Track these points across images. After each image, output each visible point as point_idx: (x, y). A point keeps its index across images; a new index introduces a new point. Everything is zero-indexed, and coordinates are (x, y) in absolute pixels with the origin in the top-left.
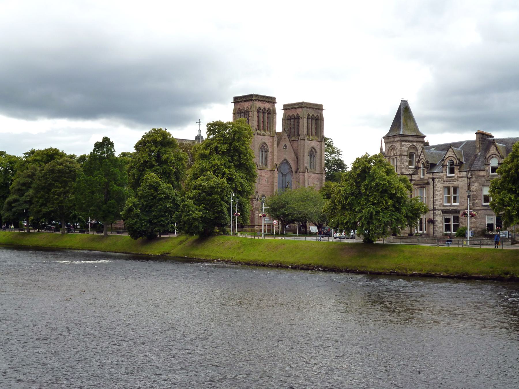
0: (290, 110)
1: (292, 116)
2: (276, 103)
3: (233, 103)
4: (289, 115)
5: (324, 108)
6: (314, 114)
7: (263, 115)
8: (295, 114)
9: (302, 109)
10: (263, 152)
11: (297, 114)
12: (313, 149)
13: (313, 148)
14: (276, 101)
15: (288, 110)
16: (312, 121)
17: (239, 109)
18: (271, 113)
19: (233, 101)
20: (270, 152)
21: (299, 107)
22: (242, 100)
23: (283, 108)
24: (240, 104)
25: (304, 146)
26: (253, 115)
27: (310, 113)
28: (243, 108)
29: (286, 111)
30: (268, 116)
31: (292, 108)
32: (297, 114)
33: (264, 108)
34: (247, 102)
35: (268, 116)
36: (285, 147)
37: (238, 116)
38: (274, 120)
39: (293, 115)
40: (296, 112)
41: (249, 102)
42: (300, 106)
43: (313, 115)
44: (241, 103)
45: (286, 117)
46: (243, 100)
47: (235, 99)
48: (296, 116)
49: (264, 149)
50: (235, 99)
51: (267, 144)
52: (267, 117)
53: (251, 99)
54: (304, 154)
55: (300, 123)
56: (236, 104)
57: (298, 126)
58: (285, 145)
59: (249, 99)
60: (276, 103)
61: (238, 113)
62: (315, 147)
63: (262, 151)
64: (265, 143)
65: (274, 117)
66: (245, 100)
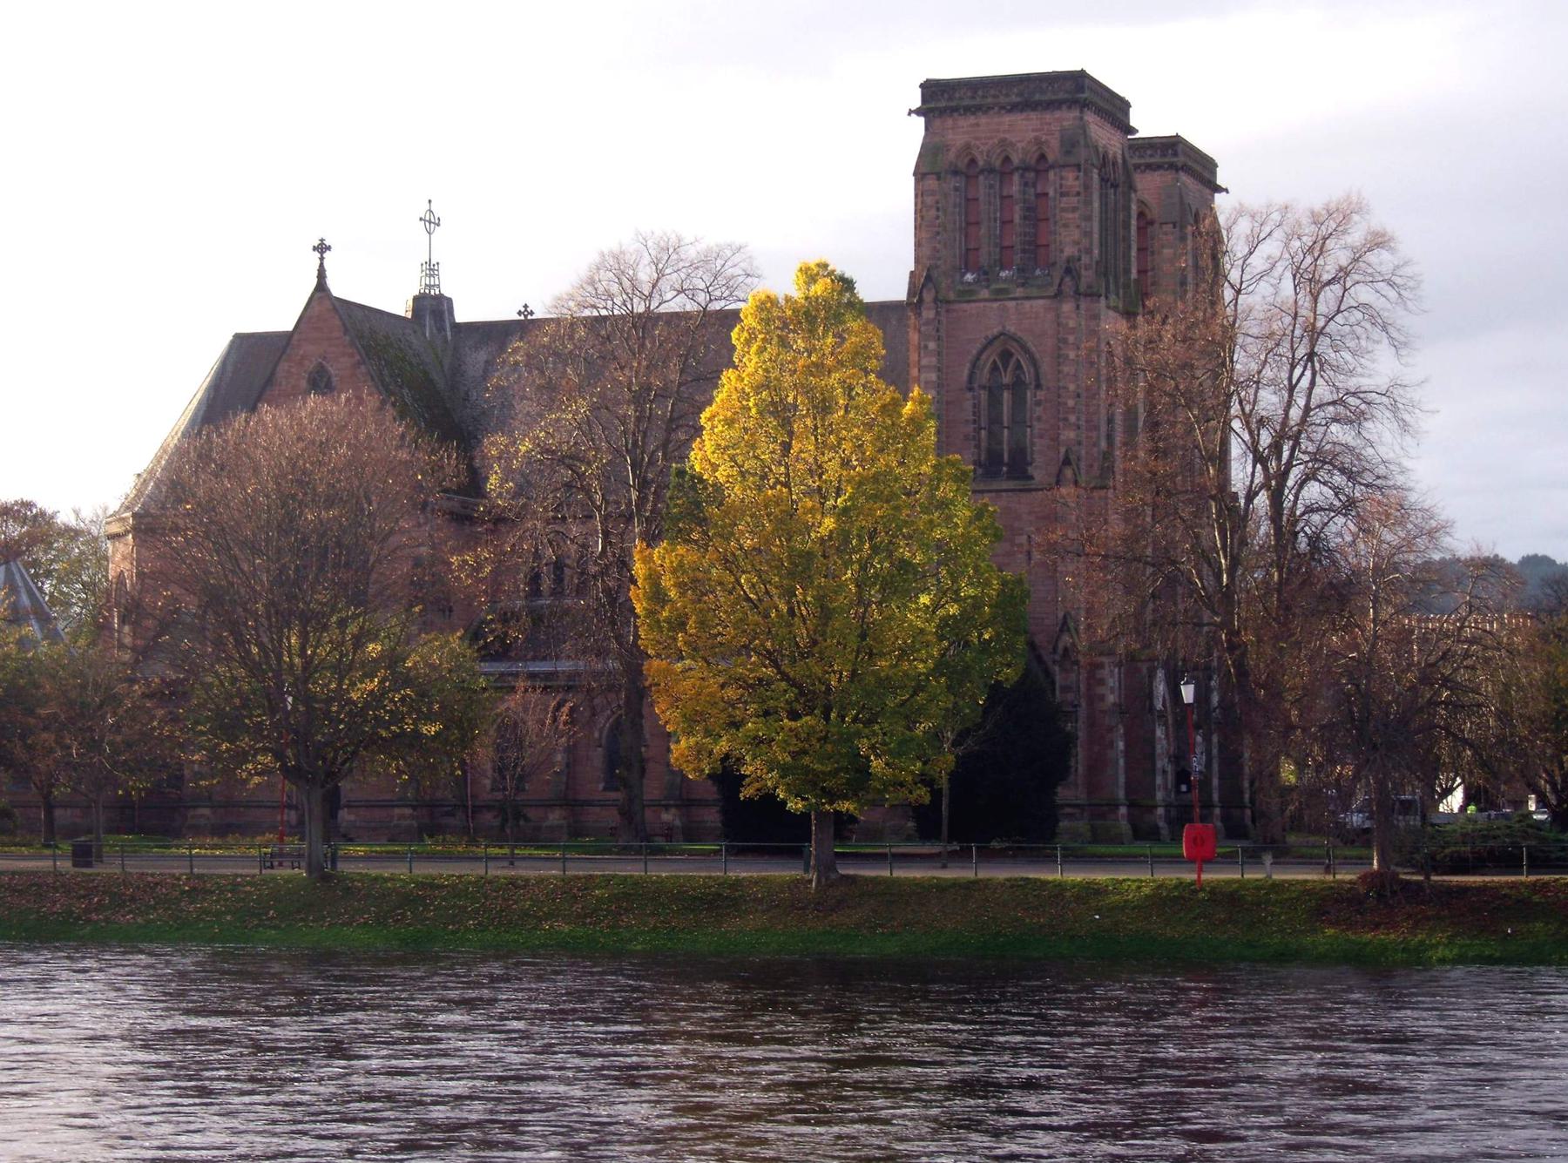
3: (918, 112)
9: (1169, 176)
17: (968, 147)
19: (917, 103)
22: (990, 100)
24: (972, 120)
26: (1087, 187)
28: (1003, 141)
34: (1033, 115)
37: (956, 189)
41: (1048, 116)
42: (1157, 159)
46: (1002, 100)
47: (932, 89)
50: (932, 89)
53: (1061, 96)
56: (937, 123)
59: (1049, 96)
61: (956, 173)
66: (1015, 99)
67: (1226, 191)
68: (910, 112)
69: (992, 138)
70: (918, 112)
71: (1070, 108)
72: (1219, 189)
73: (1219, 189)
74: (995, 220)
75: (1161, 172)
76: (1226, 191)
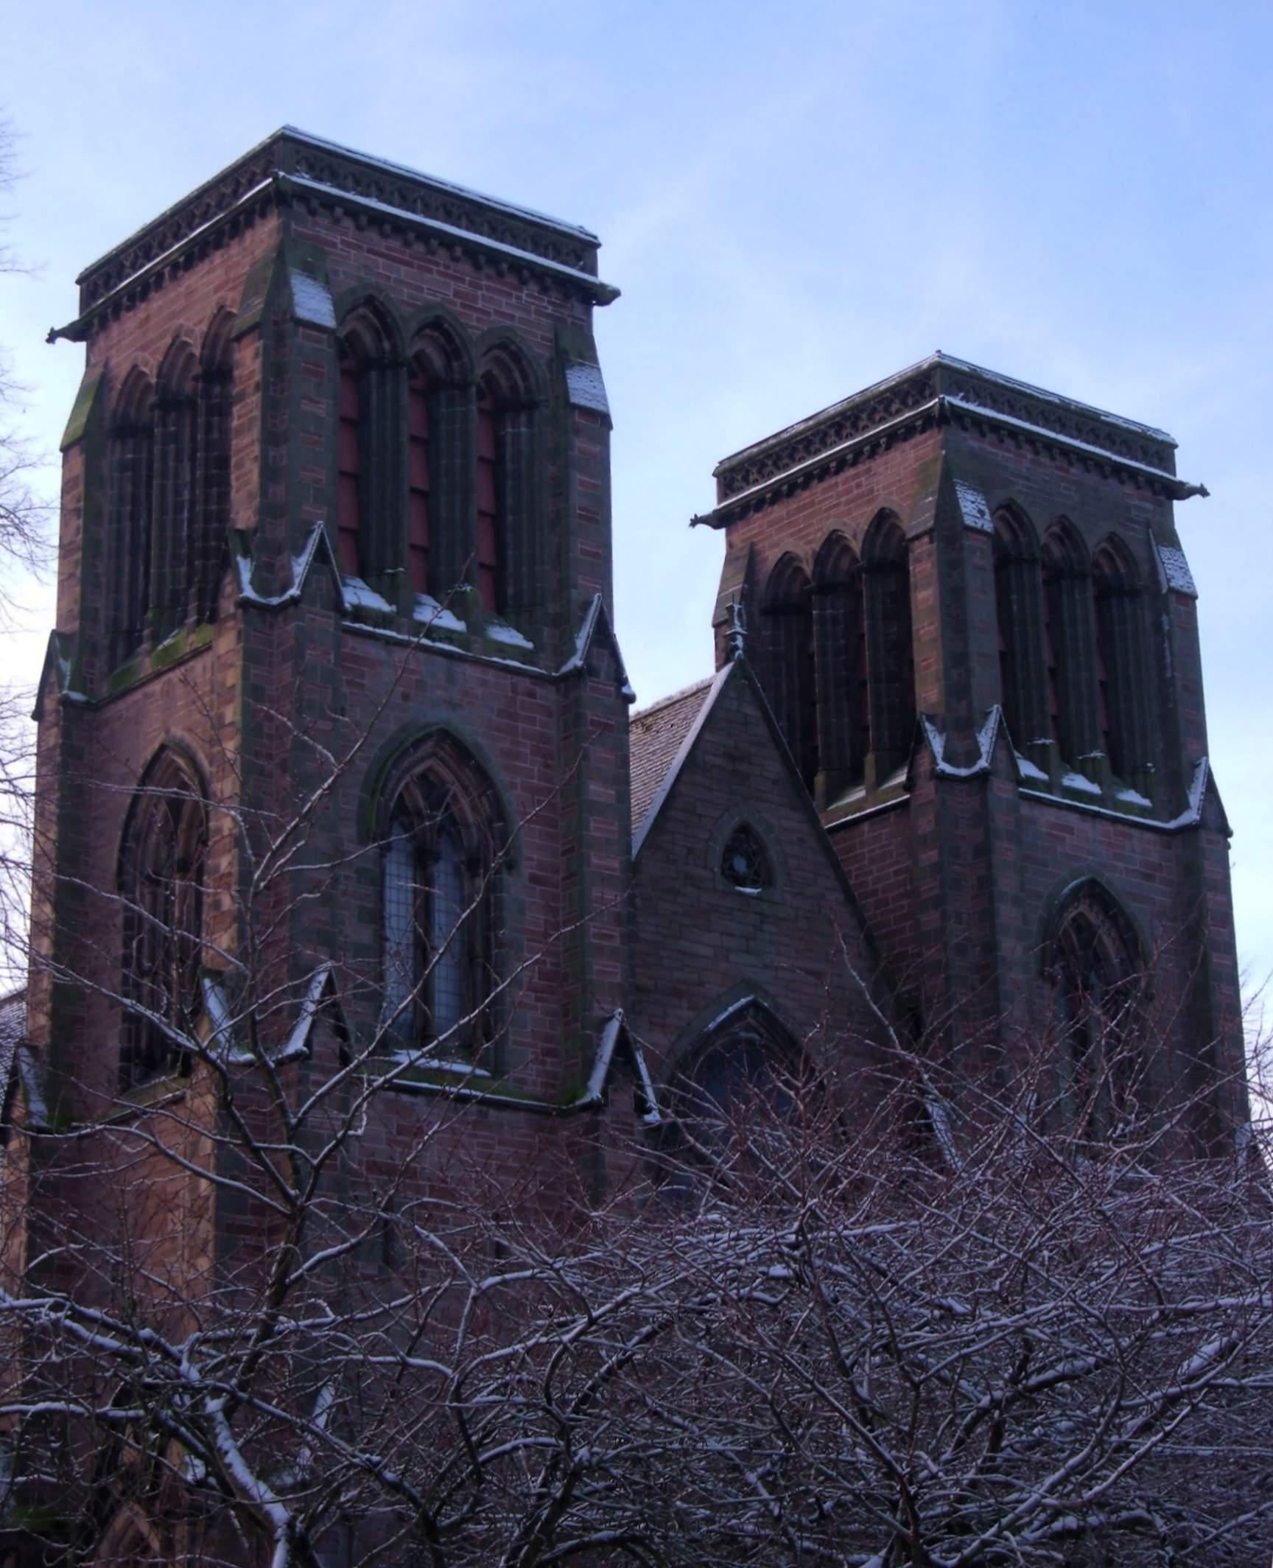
0: (804, 496)
1: (820, 559)
2: (606, 296)
3: (74, 332)
4: (787, 560)
5: (1185, 472)
6: (1074, 518)
7: (431, 421)
8: (855, 525)
10: (442, 871)
11: (884, 519)
12: (1094, 917)
13: (1094, 891)
14: (607, 273)
15: (778, 511)
16: (1054, 607)
18: (530, 406)
20: (526, 869)
21: (895, 437)
23: (709, 501)
24: (142, 310)
25: (984, 851)
27: (1020, 500)
29: (757, 522)
30: (499, 444)
31: (822, 472)
32: (884, 519)
33: (438, 325)
34: (217, 257)
35: (499, 444)
36: (740, 865)
38: (577, 476)
39: (834, 540)
40: (870, 495)
43: (1067, 533)
44: (157, 302)
45: (762, 587)
48: (870, 537)
49: (452, 826)
51: (501, 776)
52: (481, 446)
54: (990, 947)
55: (925, 596)
57: (902, 646)
58: (744, 839)
60: (606, 296)
62: (1118, 880)
63: (422, 860)
64: (463, 753)
65: (579, 443)
67: (1203, 492)
68: (52, 336)
69: (162, 337)
70: (74, 332)
71: (263, 215)
72: (1183, 492)
73: (1183, 492)
74: (178, 509)
75: (918, 438)
76: (1203, 492)
